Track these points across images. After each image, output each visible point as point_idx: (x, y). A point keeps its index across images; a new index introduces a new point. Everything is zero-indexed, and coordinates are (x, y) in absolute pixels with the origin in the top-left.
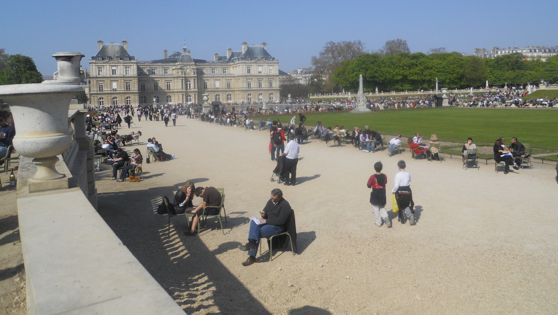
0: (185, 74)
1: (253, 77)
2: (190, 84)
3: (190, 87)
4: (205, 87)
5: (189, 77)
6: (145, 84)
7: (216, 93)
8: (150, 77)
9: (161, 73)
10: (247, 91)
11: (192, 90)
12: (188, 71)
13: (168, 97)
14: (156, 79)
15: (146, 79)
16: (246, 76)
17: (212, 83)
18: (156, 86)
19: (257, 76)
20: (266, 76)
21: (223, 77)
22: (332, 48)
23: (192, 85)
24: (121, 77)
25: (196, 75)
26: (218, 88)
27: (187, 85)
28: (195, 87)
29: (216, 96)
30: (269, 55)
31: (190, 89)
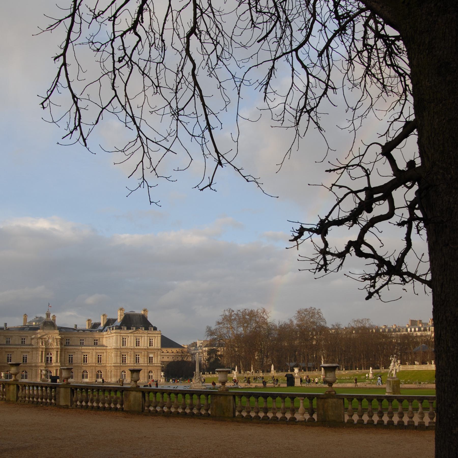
2: (51, 358)
3: (51, 360)
9: (17, 343)
10: (121, 366)
11: (54, 364)
12: (50, 341)
16: (121, 349)
20: (145, 349)
21: (93, 349)
22: (231, 316)
23: (54, 358)
25: (59, 347)
27: (48, 358)
28: (57, 361)
30: (151, 324)
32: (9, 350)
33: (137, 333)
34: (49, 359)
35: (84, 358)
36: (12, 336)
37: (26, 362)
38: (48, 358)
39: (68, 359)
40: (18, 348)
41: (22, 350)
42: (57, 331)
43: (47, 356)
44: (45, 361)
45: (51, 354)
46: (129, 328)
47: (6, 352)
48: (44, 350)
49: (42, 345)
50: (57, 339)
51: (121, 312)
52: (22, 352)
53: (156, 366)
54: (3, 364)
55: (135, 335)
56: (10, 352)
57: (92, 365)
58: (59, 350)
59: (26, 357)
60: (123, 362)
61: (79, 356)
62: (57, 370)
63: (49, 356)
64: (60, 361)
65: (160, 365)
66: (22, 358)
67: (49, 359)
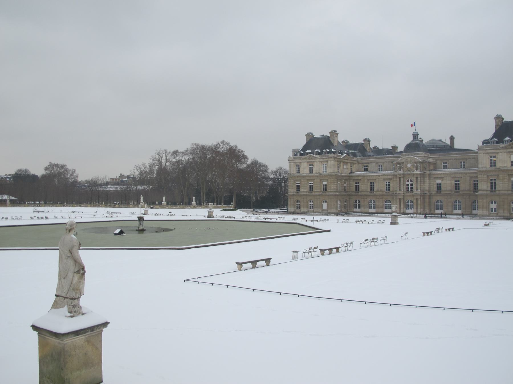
2: (412, 185)
3: (412, 188)
6: (360, 184)
15: (360, 178)
21: (466, 173)
23: (414, 186)
24: (317, 176)
27: (408, 185)
31: (412, 191)
32: (371, 178)
35: (456, 184)
36: (383, 163)
37: (389, 190)
38: (408, 185)
39: (435, 186)
40: (379, 176)
41: (384, 177)
43: (407, 183)
47: (368, 180)
48: (401, 176)
52: (384, 179)
54: (365, 193)
55: (508, 150)
56: (373, 179)
57: (465, 192)
58: (418, 176)
59: (389, 185)
60: (492, 188)
61: (448, 182)
62: (417, 199)
63: (409, 183)
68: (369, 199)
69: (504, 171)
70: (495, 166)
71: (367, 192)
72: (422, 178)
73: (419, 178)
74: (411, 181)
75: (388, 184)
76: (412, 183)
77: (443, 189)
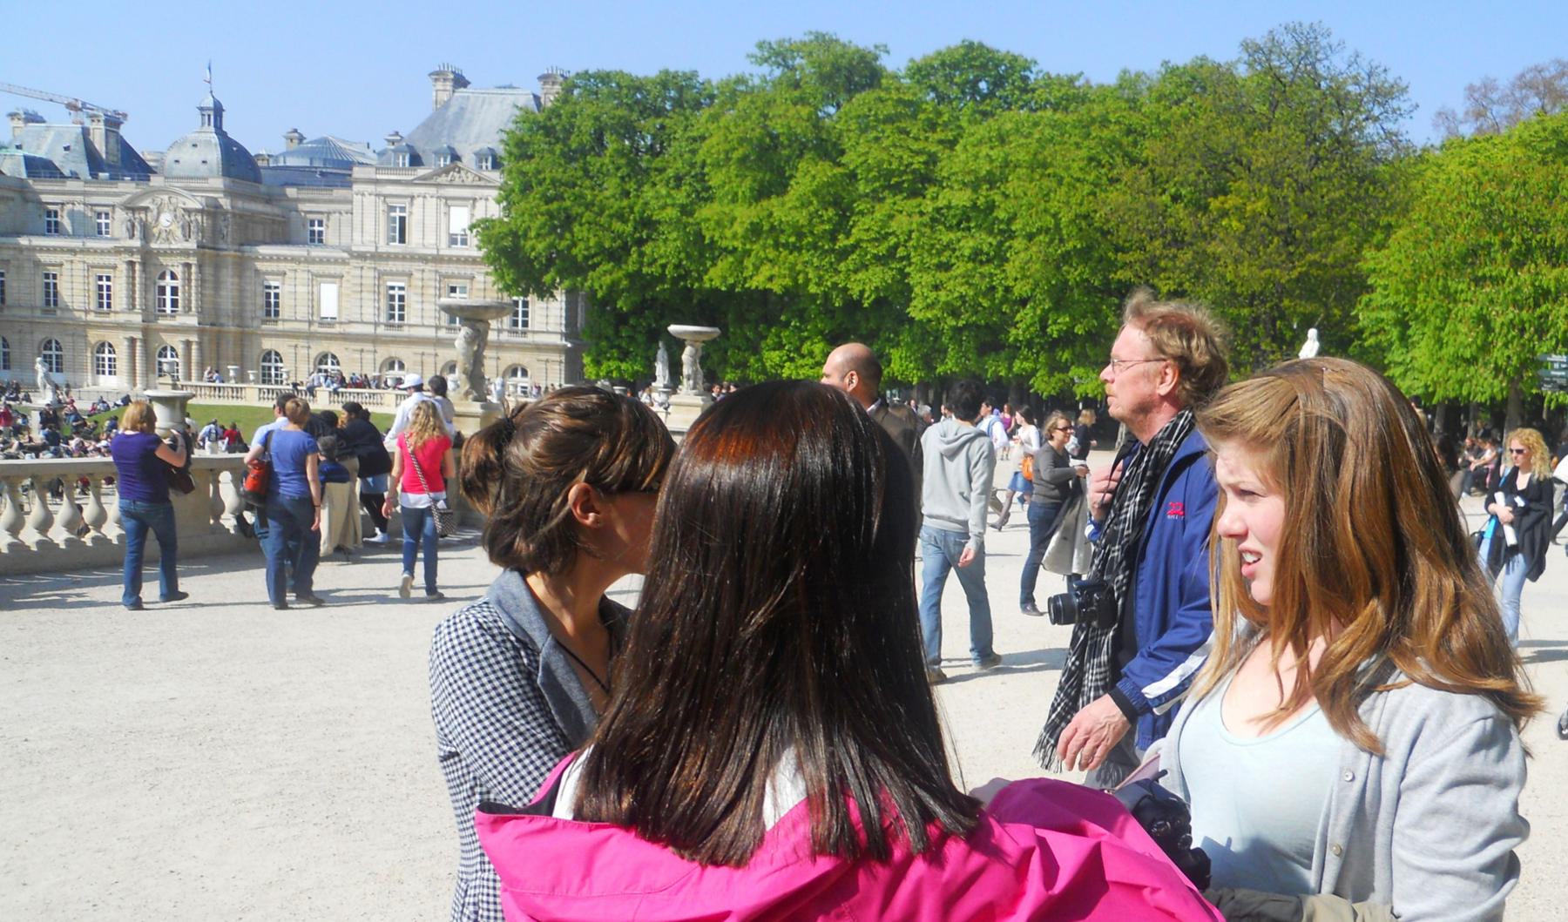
0: (146, 236)
1: (414, 267)
2: (174, 291)
4: (271, 310)
5: (166, 253)
7: (318, 348)
8: (20, 249)
12: (165, 219)
13: (101, 347)
14: (44, 258)
16: (377, 257)
17: (302, 290)
18: (51, 295)
19: (438, 259)
23: (180, 297)
25: (192, 245)
26: (331, 322)
27: (162, 290)
28: (188, 310)
29: (323, 359)
33: (451, 185)
34: (168, 297)
39: (261, 301)
40: (73, 251)
42: (218, 182)
43: (162, 283)
44: (145, 311)
45: (173, 277)
46: (416, 161)
48: (137, 258)
49: (132, 236)
50: (188, 211)
51: (440, 85)
53: (539, 348)
58: (193, 260)
62: (188, 344)
64: (201, 313)
65: (557, 340)
66: (93, 288)
67: (168, 297)
68: (40, 336)
69: (424, 259)
70: (402, 240)
71: (32, 308)
72: (208, 270)
73: (194, 269)
74: (173, 277)
75: (104, 283)
76: (174, 283)
77: (285, 312)
